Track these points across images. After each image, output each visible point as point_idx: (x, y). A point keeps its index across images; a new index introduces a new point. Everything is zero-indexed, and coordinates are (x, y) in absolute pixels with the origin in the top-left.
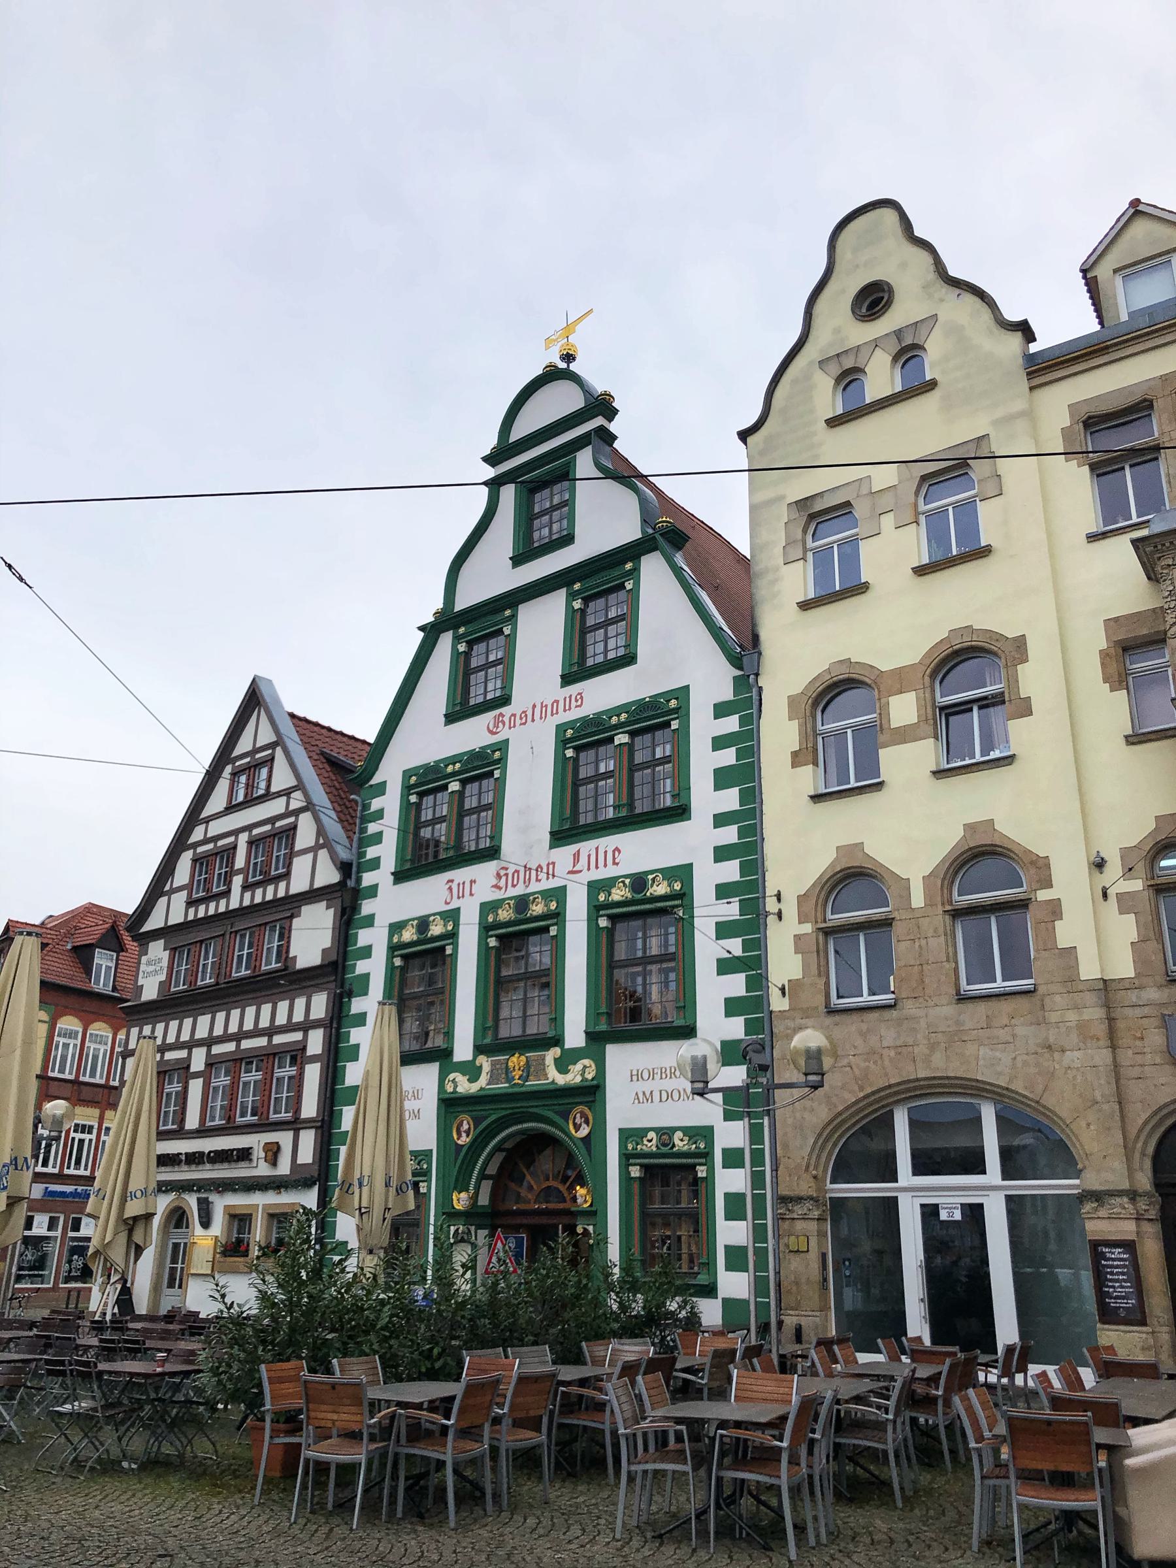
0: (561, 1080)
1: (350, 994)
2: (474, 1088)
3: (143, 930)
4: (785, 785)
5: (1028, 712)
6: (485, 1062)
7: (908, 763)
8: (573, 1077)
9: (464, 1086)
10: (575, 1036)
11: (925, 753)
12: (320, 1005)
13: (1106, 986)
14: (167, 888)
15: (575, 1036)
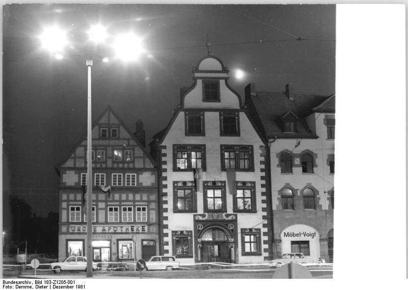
0: (226, 219)
1: (162, 196)
2: (204, 219)
3: (63, 166)
4: (276, 170)
5: (317, 167)
6: (207, 214)
7: (297, 170)
8: (230, 218)
9: (201, 218)
10: (230, 210)
11: (301, 169)
12: (153, 197)
13: (326, 210)
14: (73, 155)
15: (230, 210)
